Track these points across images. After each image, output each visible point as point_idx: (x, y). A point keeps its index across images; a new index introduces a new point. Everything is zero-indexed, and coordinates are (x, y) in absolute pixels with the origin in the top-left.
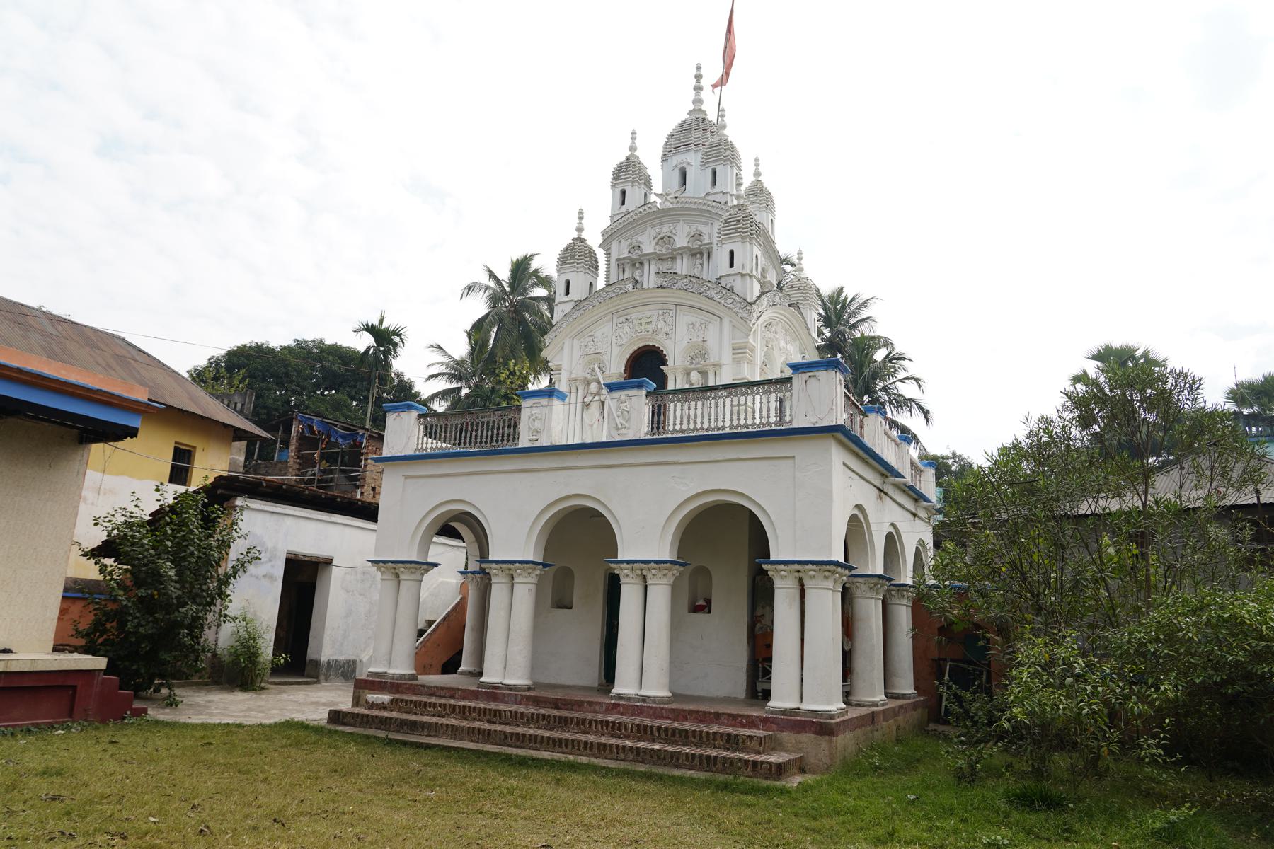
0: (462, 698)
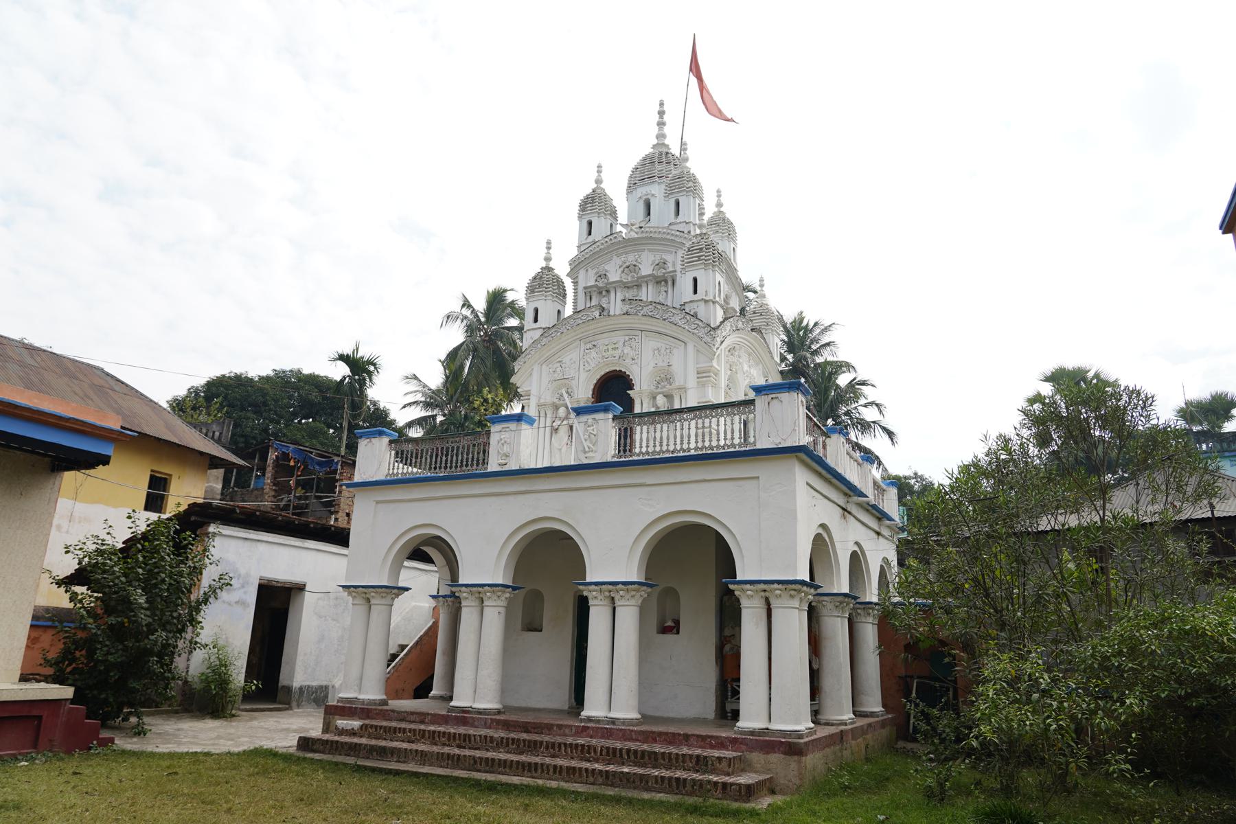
0: (432, 723)
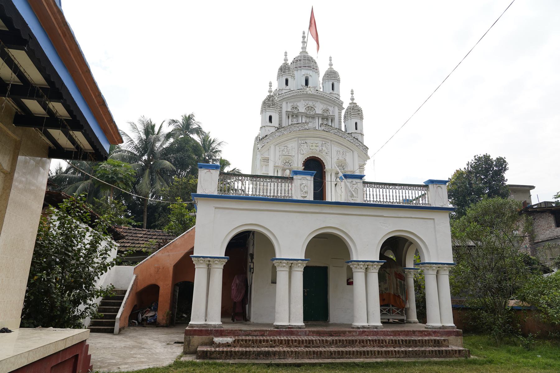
0: (270, 336)
